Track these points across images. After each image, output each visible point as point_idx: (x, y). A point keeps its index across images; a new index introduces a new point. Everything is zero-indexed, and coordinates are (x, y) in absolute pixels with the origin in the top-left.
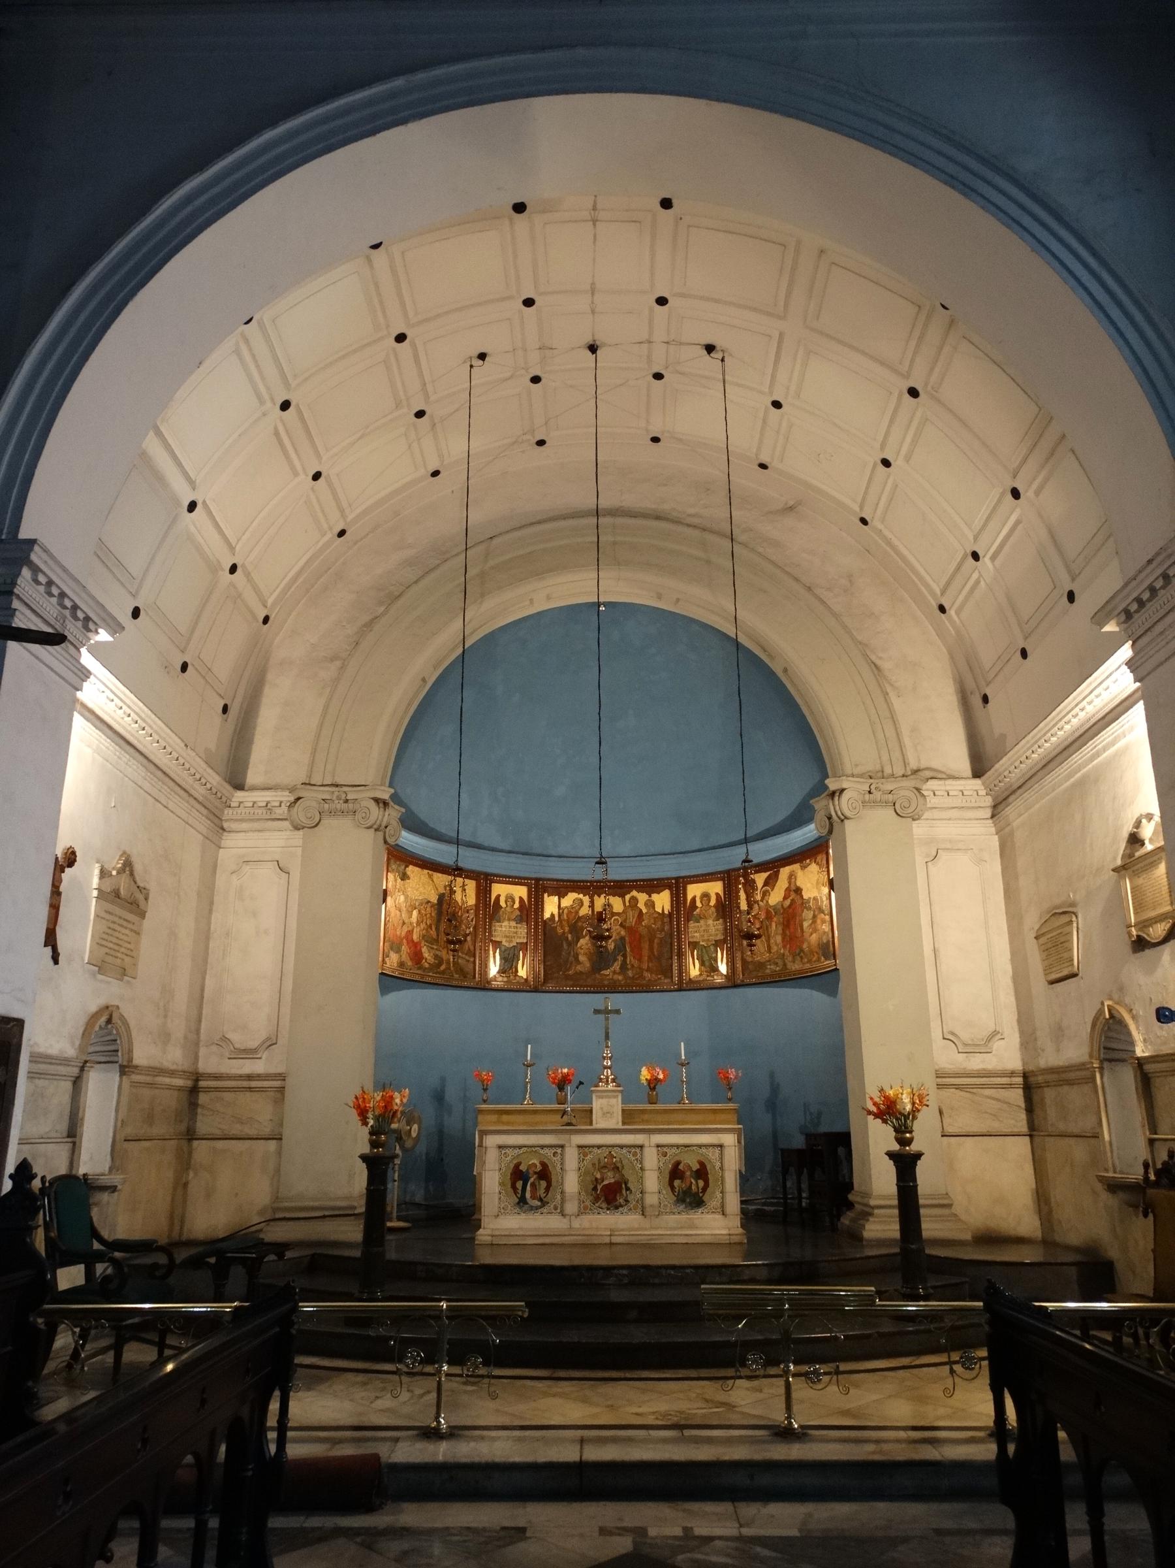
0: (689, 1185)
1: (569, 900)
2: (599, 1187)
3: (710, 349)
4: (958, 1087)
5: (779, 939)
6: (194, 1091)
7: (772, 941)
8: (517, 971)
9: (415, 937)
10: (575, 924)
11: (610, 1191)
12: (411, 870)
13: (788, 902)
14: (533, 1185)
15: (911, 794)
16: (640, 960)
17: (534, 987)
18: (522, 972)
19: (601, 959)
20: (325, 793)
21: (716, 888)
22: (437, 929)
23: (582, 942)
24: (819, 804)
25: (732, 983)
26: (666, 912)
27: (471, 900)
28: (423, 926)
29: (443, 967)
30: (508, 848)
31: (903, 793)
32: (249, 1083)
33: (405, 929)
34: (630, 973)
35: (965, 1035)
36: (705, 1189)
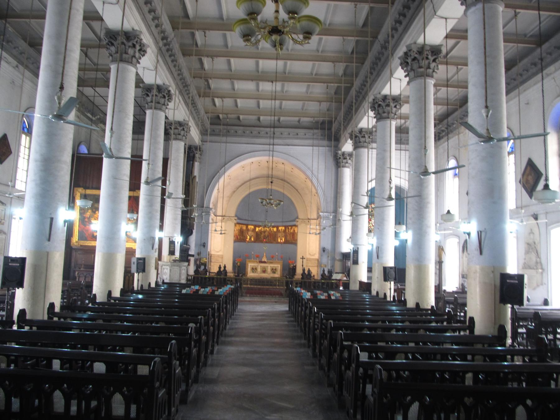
0: (274, 271)
1: (260, 228)
10: (261, 232)
11: (264, 271)
12: (237, 225)
17: (255, 242)
18: (252, 239)
21: (283, 228)
32: (218, 256)
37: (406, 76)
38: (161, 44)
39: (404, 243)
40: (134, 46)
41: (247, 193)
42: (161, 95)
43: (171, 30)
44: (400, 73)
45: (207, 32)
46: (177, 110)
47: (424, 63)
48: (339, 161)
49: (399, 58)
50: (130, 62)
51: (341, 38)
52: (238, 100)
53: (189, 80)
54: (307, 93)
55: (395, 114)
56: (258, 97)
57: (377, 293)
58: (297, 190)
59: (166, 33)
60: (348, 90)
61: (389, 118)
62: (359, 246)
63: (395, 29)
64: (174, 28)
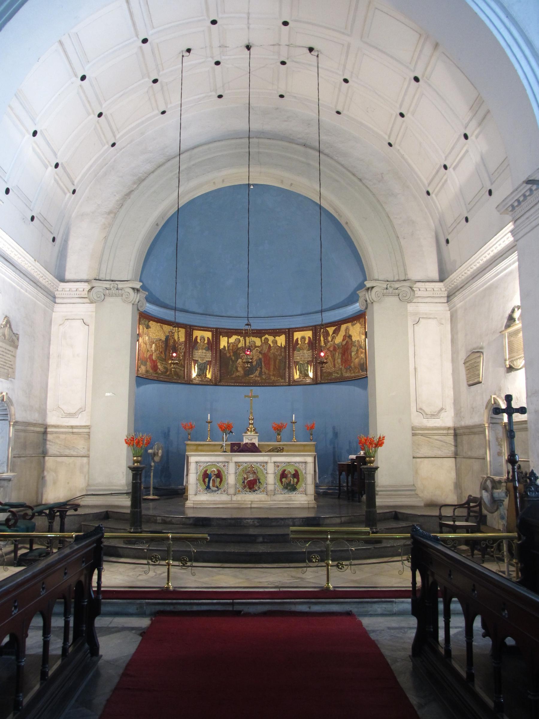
0: (289, 480)
1: (233, 339)
2: (246, 482)
3: (311, 50)
4: (422, 435)
5: (339, 361)
6: (45, 433)
7: (336, 362)
8: (206, 375)
9: (154, 358)
10: (236, 351)
11: (252, 484)
12: (152, 324)
13: (344, 343)
14: (213, 480)
15: (408, 290)
16: (269, 370)
17: (216, 382)
18: (209, 376)
20: (107, 285)
21: (309, 334)
22: (165, 354)
23: (240, 360)
24: (361, 293)
25: (316, 382)
26: (283, 346)
27: (182, 339)
28: (158, 352)
29: (168, 373)
30: (202, 312)
31: (403, 289)
32: (73, 430)
33: (149, 354)
34: (264, 377)
35: (428, 410)
36: (297, 483)
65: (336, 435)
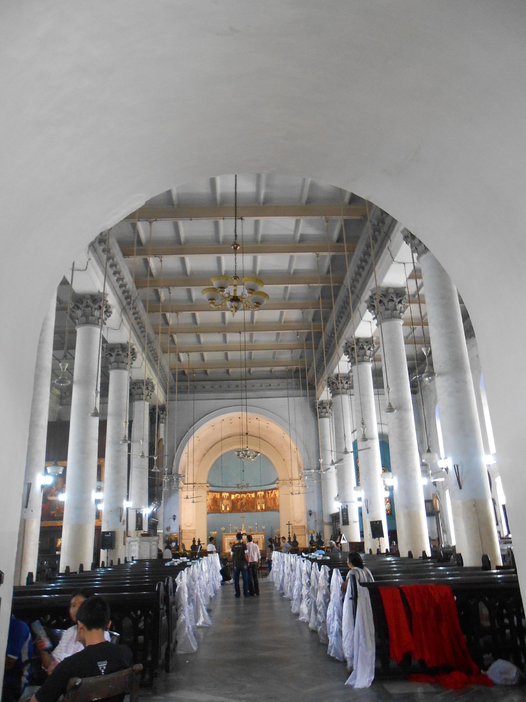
10: (237, 499)
17: (230, 512)
18: (228, 509)
19: (242, 506)
20: (199, 485)
21: (263, 493)
27: (219, 497)
32: (190, 531)
37: (374, 319)
38: (125, 303)
39: (390, 489)
40: (100, 308)
41: (219, 455)
42: (125, 354)
43: (135, 289)
44: (369, 316)
45: (171, 288)
46: (142, 368)
47: (391, 304)
48: (318, 410)
49: (366, 302)
50: (96, 324)
51: (307, 285)
52: (205, 354)
53: (153, 336)
54: (277, 341)
55: (370, 357)
56: (225, 349)
57: (370, 550)
58: (274, 448)
59: (130, 293)
60: (318, 335)
61: (364, 361)
62: (347, 504)
63: (358, 274)
64: (137, 287)
65: (272, 529)
